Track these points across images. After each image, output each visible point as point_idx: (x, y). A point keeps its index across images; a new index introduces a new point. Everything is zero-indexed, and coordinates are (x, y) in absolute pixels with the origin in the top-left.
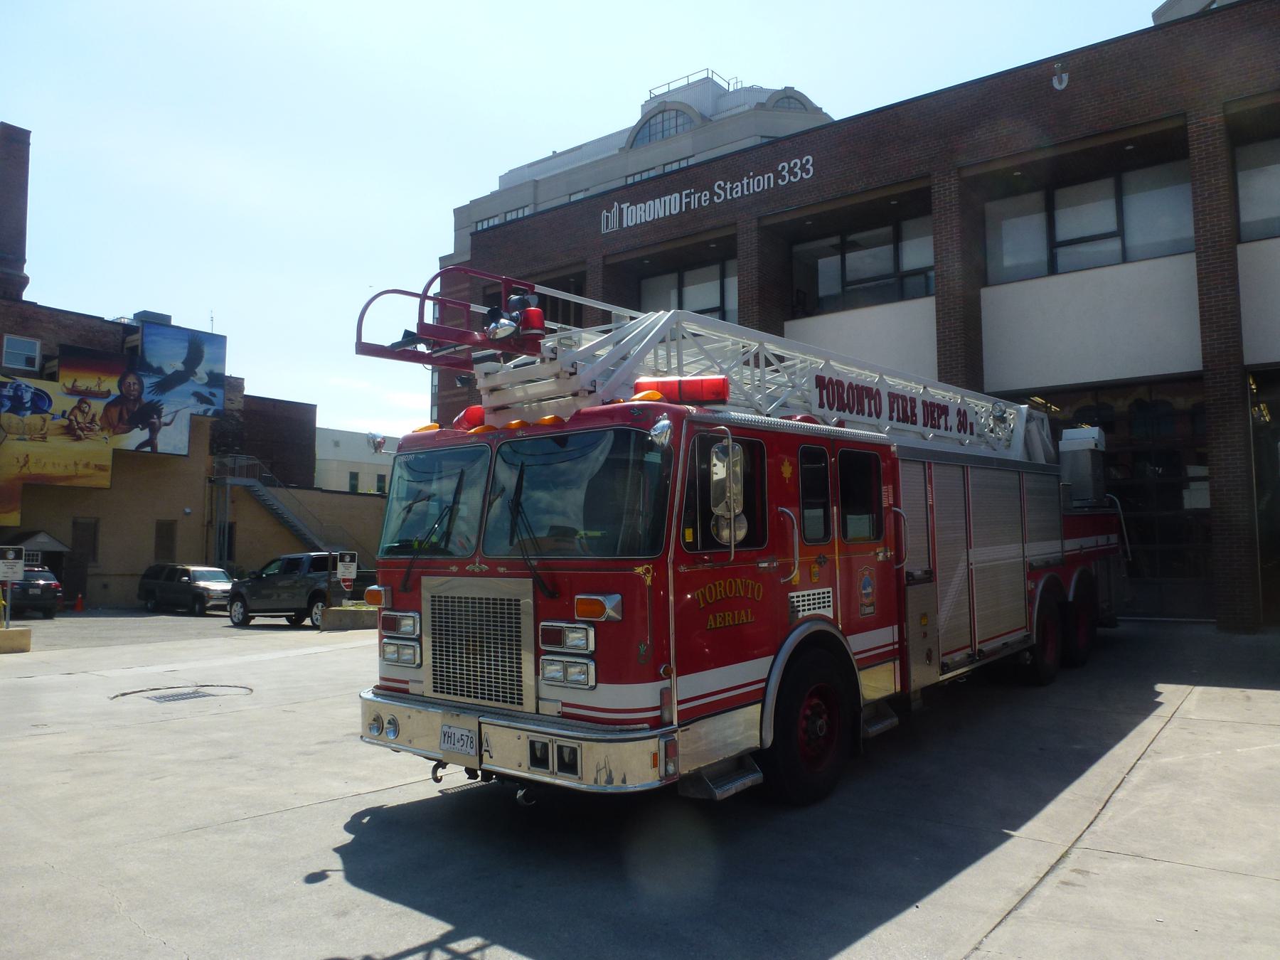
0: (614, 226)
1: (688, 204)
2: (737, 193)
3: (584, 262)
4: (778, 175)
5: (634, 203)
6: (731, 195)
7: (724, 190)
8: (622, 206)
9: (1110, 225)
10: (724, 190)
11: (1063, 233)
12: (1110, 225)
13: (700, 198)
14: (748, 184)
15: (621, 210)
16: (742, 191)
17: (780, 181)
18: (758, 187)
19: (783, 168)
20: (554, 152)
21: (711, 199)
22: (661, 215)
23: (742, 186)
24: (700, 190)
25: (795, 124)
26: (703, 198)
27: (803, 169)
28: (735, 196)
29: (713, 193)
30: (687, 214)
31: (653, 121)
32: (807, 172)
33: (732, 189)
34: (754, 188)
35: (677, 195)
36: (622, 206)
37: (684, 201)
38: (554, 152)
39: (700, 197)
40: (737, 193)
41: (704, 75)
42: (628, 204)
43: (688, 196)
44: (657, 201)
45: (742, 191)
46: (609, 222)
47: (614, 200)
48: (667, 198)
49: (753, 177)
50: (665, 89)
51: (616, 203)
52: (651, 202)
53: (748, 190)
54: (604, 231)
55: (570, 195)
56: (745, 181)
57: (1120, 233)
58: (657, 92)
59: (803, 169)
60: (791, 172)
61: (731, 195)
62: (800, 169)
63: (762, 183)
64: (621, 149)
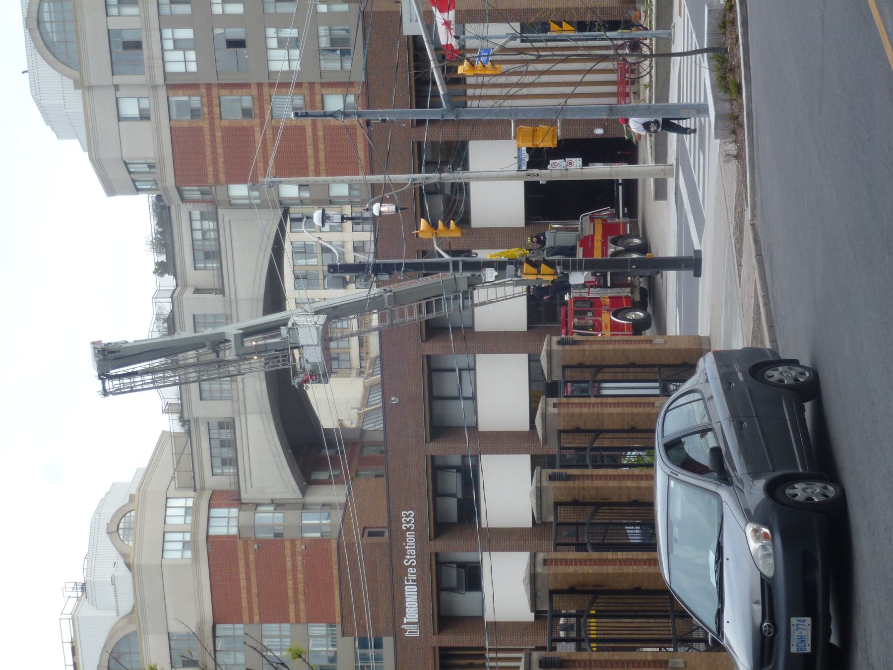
0: (415, 628)
1: (413, 581)
2: (413, 552)
3: (434, 648)
4: (408, 529)
5: (404, 614)
6: (413, 555)
7: (410, 559)
8: (405, 622)
10: (409, 560)
11: (455, 393)
13: (411, 574)
14: (409, 546)
15: (408, 623)
16: (413, 549)
17: (412, 529)
18: (413, 540)
19: (405, 527)
21: (413, 567)
22: (416, 597)
23: (409, 549)
24: (406, 574)
26: (412, 572)
27: (407, 516)
28: (415, 553)
29: (410, 566)
30: (419, 582)
32: (411, 514)
33: (410, 555)
34: (412, 543)
35: (406, 587)
36: (405, 622)
39: (411, 574)
40: (413, 552)
42: (405, 618)
43: (408, 581)
44: (407, 600)
45: (413, 549)
47: (400, 627)
48: (407, 593)
51: (402, 627)
52: (407, 604)
53: (413, 546)
54: (417, 635)
56: (407, 547)
59: (407, 516)
60: (408, 523)
61: (413, 555)
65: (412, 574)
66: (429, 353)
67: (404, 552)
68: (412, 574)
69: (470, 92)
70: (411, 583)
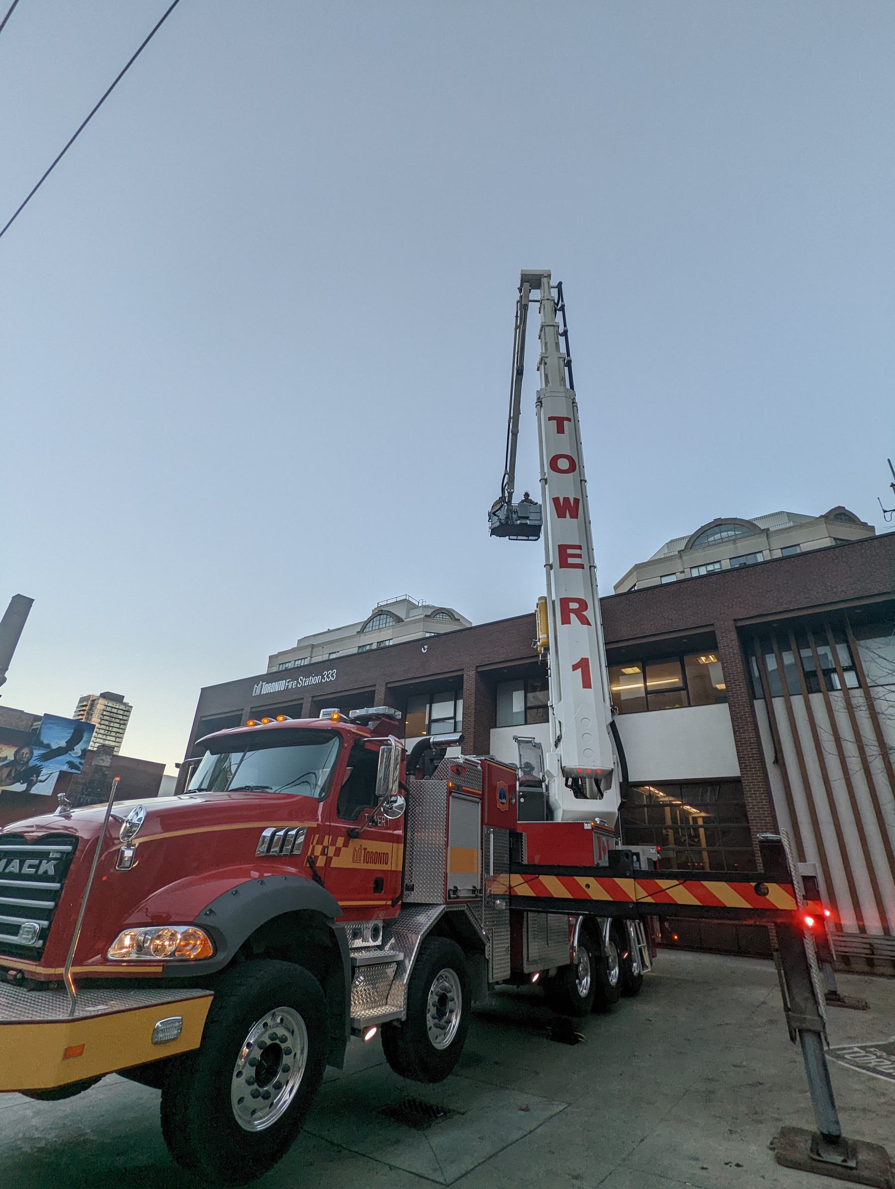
0: (258, 692)
1: (288, 686)
4: (323, 678)
5: (267, 683)
9: (452, 715)
12: (453, 715)
15: (262, 685)
20: (329, 629)
21: (297, 685)
25: (444, 627)
27: (332, 676)
29: (298, 682)
30: (287, 690)
31: (375, 619)
33: (305, 681)
37: (287, 684)
38: (329, 629)
41: (404, 598)
43: (288, 682)
46: (256, 691)
49: (314, 677)
50: (385, 603)
54: (254, 695)
55: (330, 654)
57: (454, 718)
58: (382, 604)
59: (332, 676)
62: (330, 675)
63: (315, 680)
64: (357, 632)
65: (292, 684)
66: (465, 676)
67: (307, 677)
68: (292, 684)
69: (797, 701)
70: (287, 684)
